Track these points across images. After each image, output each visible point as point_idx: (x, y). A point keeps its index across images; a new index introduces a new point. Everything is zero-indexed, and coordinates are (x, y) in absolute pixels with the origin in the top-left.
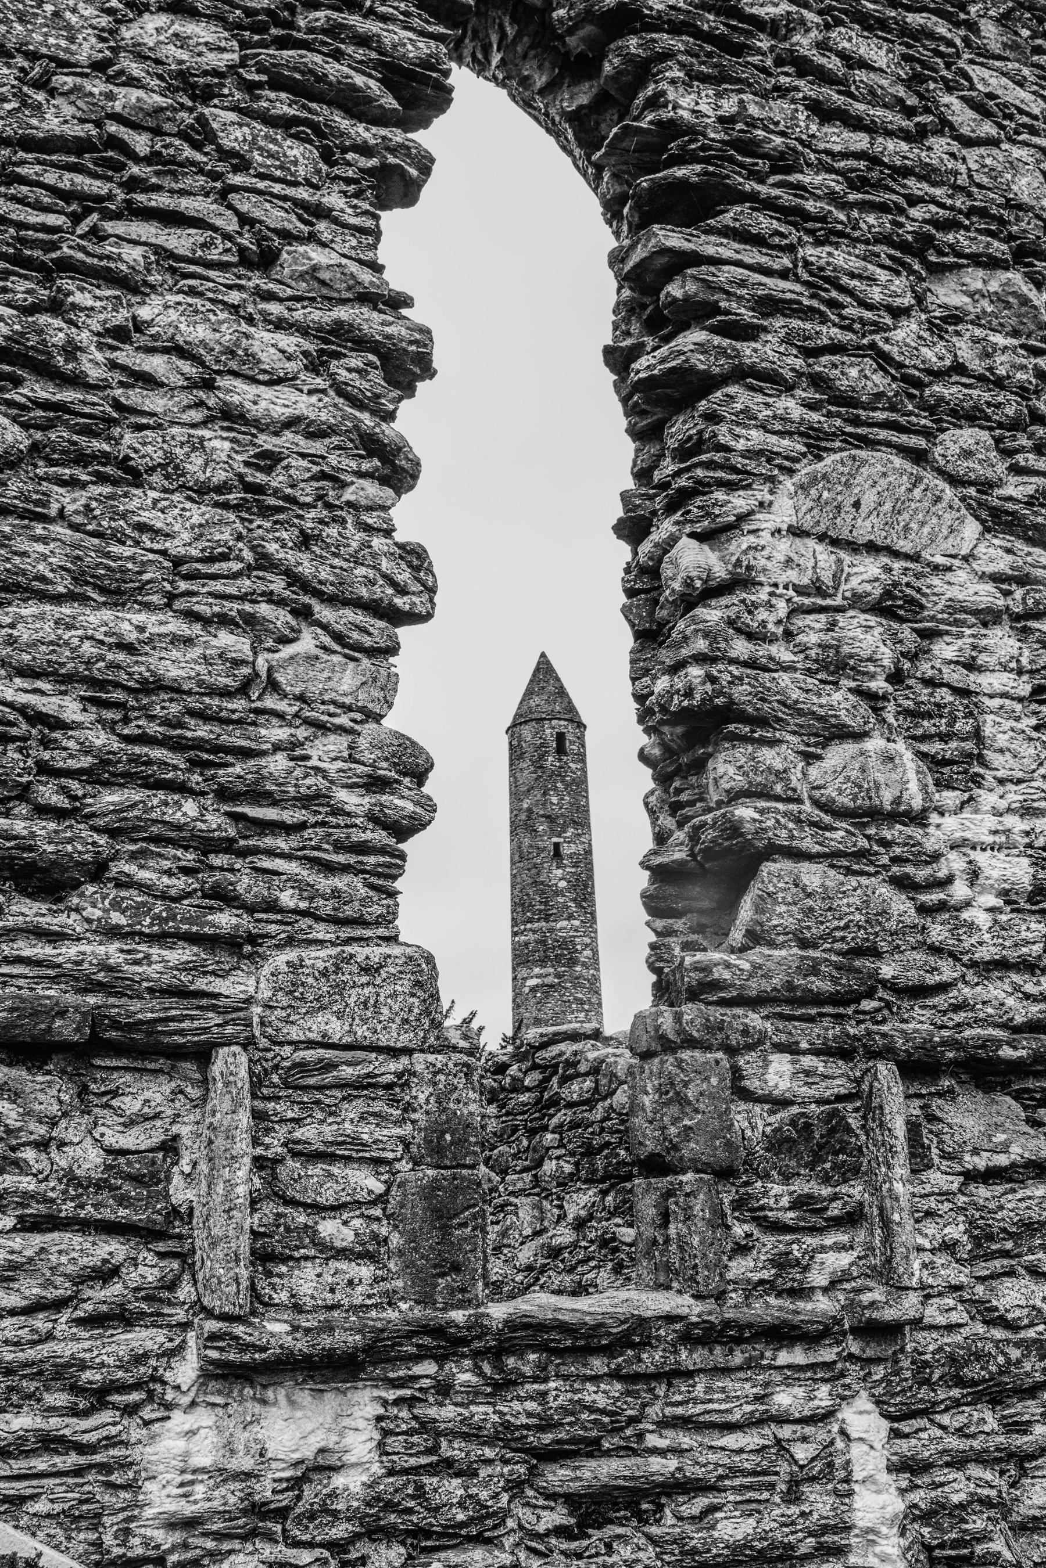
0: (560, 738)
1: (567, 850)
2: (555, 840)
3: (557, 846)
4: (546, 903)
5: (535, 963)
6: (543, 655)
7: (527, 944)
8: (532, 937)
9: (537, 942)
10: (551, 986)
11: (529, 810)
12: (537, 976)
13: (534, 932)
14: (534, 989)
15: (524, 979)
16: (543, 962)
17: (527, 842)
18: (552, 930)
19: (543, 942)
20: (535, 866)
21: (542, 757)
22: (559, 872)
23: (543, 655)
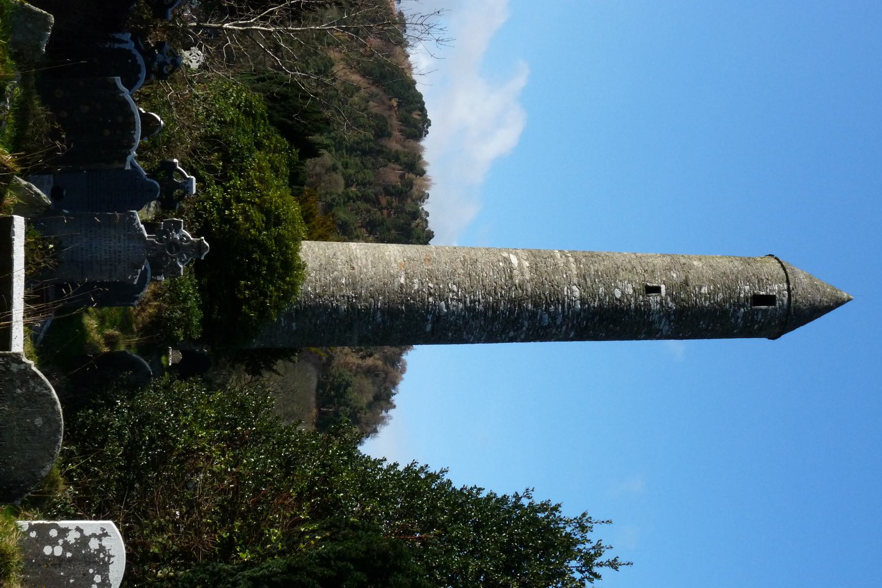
0: (770, 300)
1: (653, 299)
2: (663, 287)
3: (657, 290)
8: (561, 262)
10: (511, 277)
12: (520, 264)
13: (567, 264)
14: (506, 260)
15: (516, 254)
16: (534, 268)
21: (748, 280)
22: (631, 291)
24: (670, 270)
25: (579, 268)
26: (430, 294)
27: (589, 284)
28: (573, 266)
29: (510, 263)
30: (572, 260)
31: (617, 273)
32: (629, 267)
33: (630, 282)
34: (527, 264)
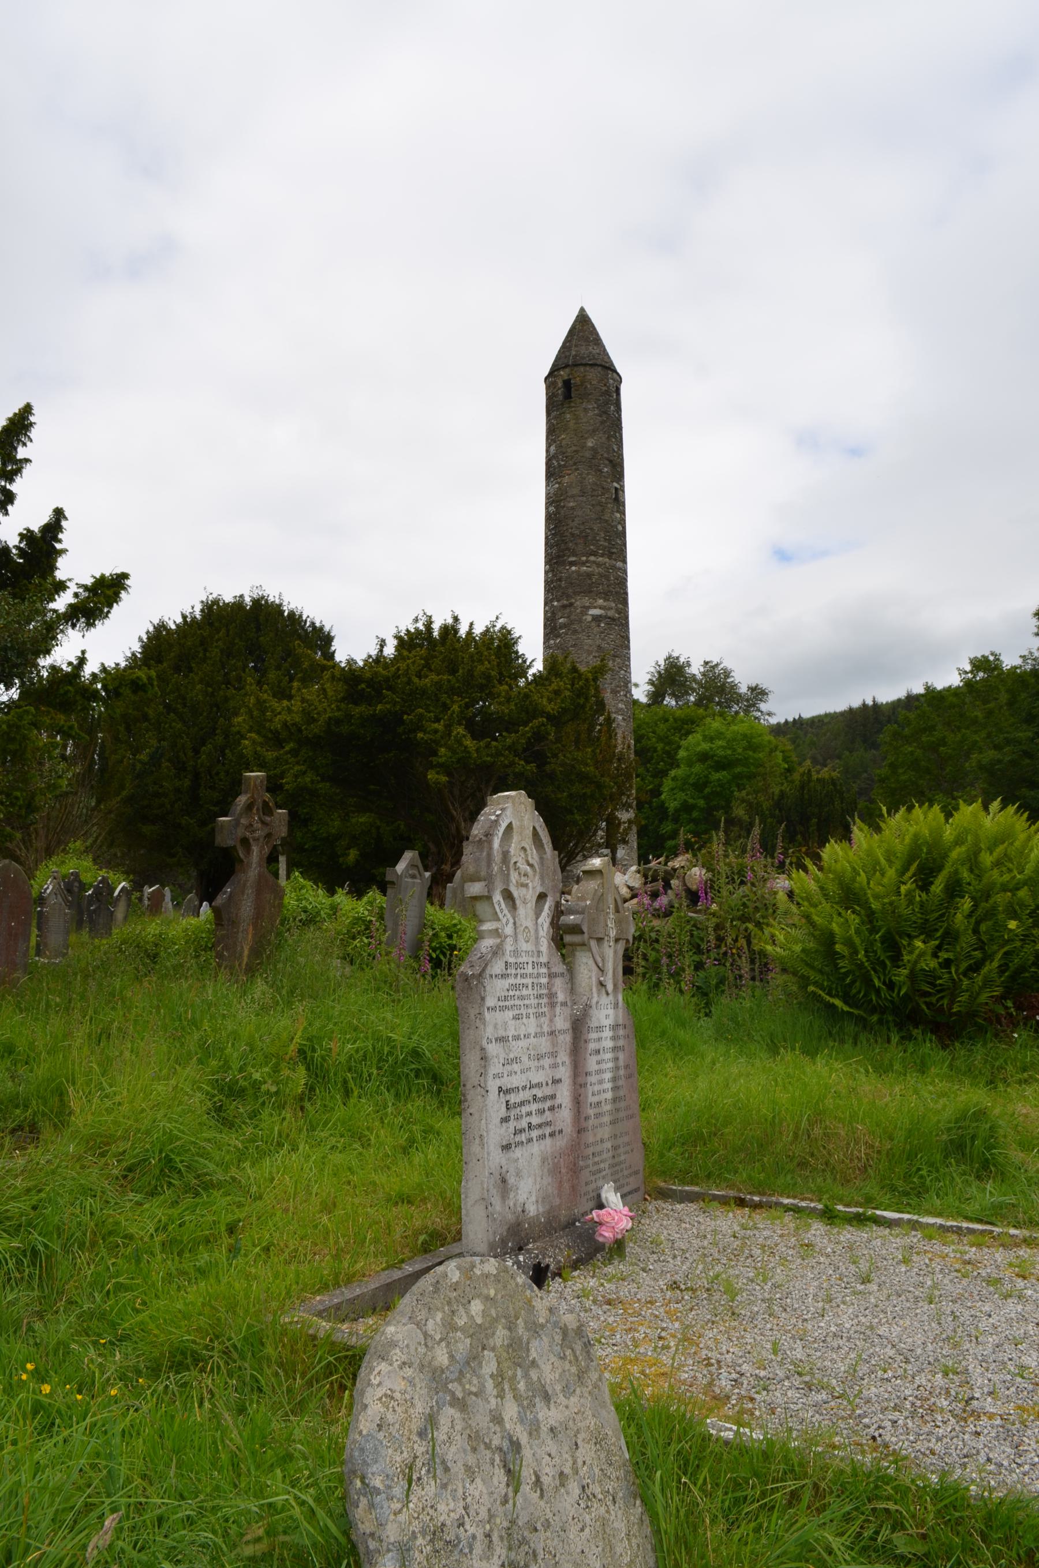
2: (616, 485)
3: (616, 489)
4: (609, 541)
5: (599, 594)
6: (582, 310)
7: (589, 575)
9: (600, 575)
10: (613, 619)
11: (592, 449)
13: (599, 565)
14: (597, 619)
15: (588, 608)
17: (591, 479)
18: (613, 567)
19: (607, 578)
20: (600, 504)
21: (607, 403)
23: (582, 310)
24: (600, 471)
25: (602, 555)
26: (625, 696)
27: (614, 550)
28: (600, 559)
29: (600, 616)
30: (592, 558)
31: (606, 521)
32: (599, 508)
33: (612, 513)
34: (601, 602)
